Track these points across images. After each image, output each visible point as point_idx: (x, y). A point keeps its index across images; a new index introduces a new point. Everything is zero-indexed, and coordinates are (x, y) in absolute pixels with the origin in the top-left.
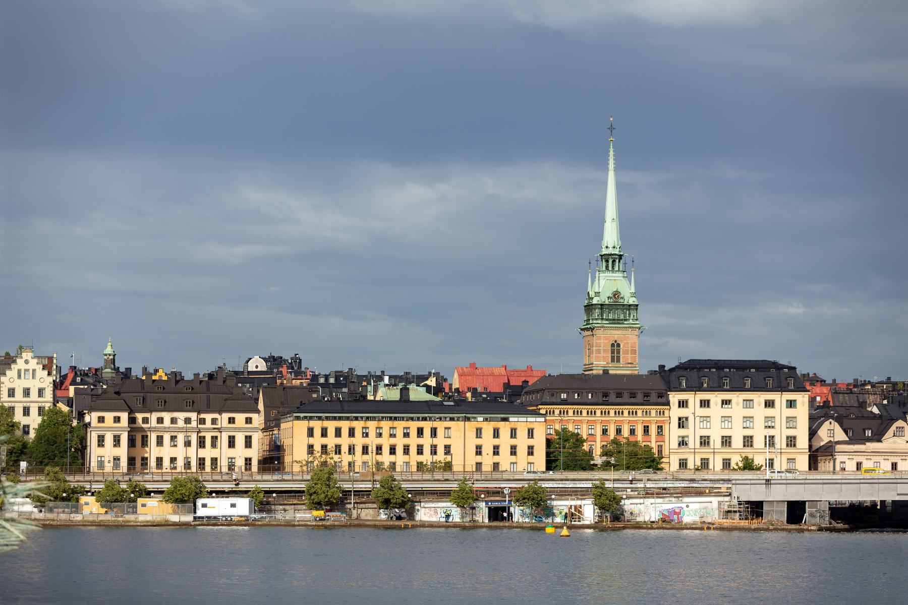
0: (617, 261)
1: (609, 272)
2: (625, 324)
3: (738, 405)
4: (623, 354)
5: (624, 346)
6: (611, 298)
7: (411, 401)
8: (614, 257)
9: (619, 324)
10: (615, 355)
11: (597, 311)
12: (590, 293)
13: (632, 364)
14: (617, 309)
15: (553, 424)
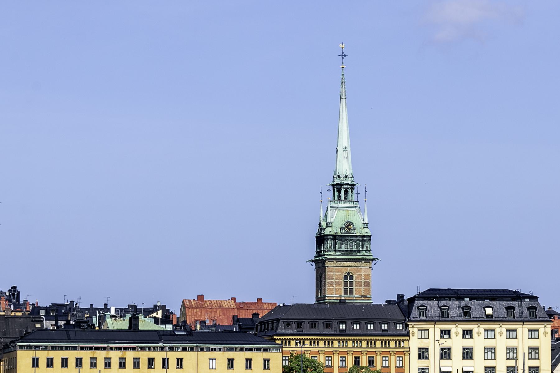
0: (350, 191)
1: (341, 202)
2: (358, 255)
3: (479, 336)
4: (356, 286)
5: (357, 278)
6: (344, 229)
7: (141, 331)
8: (346, 186)
9: (352, 255)
10: (348, 287)
11: (329, 242)
12: (322, 223)
13: (366, 297)
14: (351, 240)
15: (389, 356)
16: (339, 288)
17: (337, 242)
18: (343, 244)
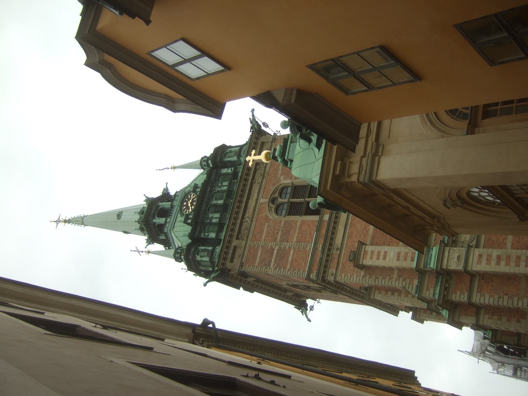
11: (198, 258)
16: (297, 231)
17: (204, 235)
18: (212, 218)
